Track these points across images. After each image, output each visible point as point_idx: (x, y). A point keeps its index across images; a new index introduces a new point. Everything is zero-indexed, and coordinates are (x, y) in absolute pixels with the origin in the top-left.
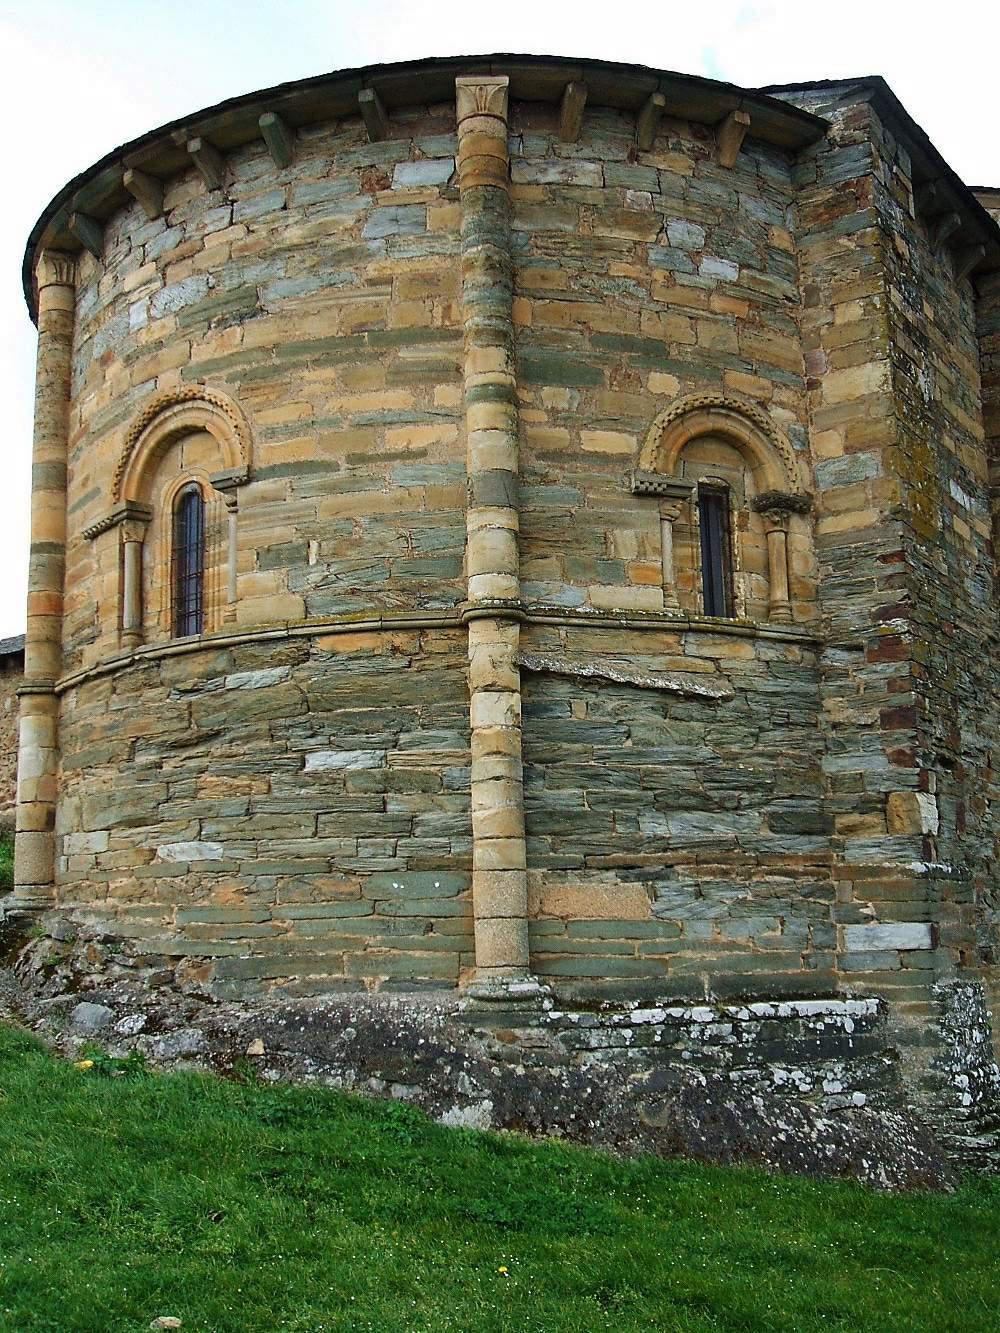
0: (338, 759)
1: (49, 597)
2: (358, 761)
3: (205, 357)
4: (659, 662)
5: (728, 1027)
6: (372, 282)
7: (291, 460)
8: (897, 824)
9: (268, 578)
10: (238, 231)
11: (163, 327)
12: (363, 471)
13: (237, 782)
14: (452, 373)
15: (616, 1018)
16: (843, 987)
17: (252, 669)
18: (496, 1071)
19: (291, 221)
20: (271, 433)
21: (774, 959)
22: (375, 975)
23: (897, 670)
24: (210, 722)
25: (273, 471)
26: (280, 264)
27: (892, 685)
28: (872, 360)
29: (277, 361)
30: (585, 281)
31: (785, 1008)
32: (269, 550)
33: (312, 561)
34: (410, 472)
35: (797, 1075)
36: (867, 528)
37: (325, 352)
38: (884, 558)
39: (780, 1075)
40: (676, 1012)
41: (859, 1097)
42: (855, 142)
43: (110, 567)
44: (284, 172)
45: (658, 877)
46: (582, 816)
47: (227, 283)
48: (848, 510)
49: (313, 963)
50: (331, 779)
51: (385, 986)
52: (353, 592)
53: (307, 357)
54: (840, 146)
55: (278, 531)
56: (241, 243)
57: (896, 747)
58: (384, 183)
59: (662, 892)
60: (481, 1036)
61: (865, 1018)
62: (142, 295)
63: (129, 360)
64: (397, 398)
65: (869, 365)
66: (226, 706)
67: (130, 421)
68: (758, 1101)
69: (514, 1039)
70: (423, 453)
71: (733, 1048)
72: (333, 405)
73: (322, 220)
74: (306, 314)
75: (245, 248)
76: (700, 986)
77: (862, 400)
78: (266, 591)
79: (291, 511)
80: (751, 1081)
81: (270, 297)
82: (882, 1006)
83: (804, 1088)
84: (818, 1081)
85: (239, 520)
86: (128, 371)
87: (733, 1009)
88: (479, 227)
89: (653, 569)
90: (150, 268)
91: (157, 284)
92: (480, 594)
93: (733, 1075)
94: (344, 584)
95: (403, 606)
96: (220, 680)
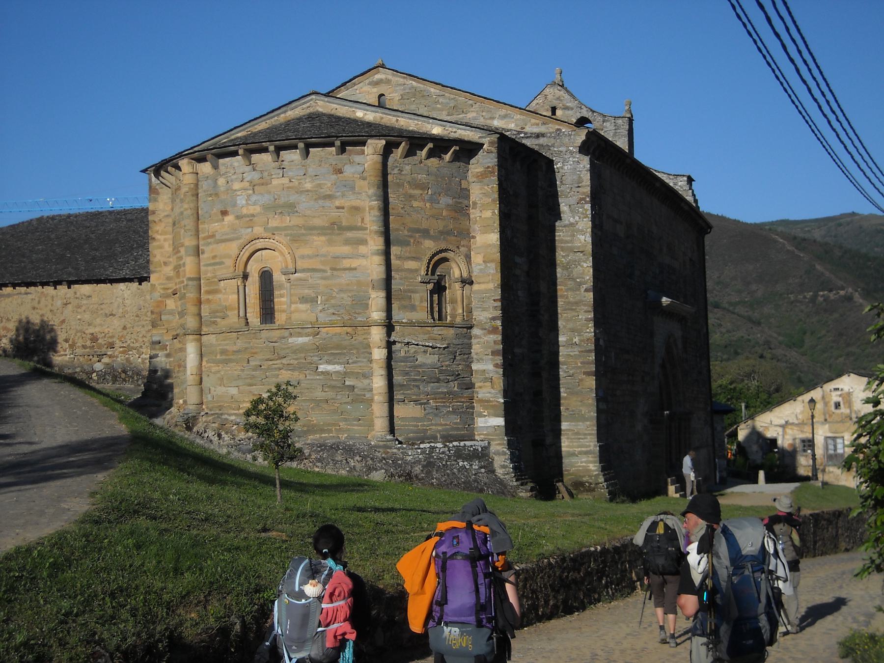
0: (330, 368)
1: (197, 298)
2: (338, 368)
3: (275, 225)
4: (426, 337)
5: (447, 449)
6: (338, 208)
7: (310, 267)
8: (495, 387)
9: (303, 307)
10: (285, 181)
11: (255, 209)
12: (335, 273)
13: (294, 373)
14: (364, 242)
15: (416, 446)
16: (477, 437)
17: (298, 337)
18: (384, 461)
19: (307, 180)
20: (303, 257)
21: (458, 429)
22: (343, 434)
23: (497, 338)
24: (282, 353)
25: (304, 271)
26: (304, 196)
27: (495, 342)
28: (493, 232)
29: (304, 232)
30: (405, 209)
31: (462, 444)
32: (303, 297)
33: (319, 303)
34: (351, 275)
35: (466, 463)
36: (489, 289)
37: (321, 231)
38: (494, 300)
39: (461, 464)
40: (432, 445)
41: (483, 470)
42: (492, 152)
43: (234, 293)
44: (304, 161)
45: (425, 404)
46: (404, 385)
47: (283, 199)
48: (483, 283)
49: (322, 431)
50: (326, 373)
51: (346, 438)
52: (333, 314)
53: (315, 232)
54: (487, 152)
55: (306, 291)
56: (287, 185)
57: (496, 362)
58: (340, 171)
59: (427, 408)
60: (379, 452)
61: (484, 447)
62: (244, 194)
63: (238, 217)
64: (346, 249)
65: (493, 234)
66: (288, 348)
67: (241, 241)
68: (455, 470)
69: (388, 452)
70: (355, 269)
71: (448, 456)
72: (324, 250)
73: (319, 182)
74: (314, 217)
75: (288, 188)
76: (437, 437)
77: (490, 245)
78: (303, 311)
79: (311, 285)
80: (453, 465)
81: (300, 208)
82: (489, 443)
83: (467, 467)
84: (471, 465)
85: (291, 286)
86: (237, 221)
87: (448, 444)
88: (375, 195)
89: (424, 307)
90: (246, 184)
91: (251, 192)
92: (376, 318)
93: (448, 463)
94: (331, 311)
95: (350, 319)
96: (286, 339)
